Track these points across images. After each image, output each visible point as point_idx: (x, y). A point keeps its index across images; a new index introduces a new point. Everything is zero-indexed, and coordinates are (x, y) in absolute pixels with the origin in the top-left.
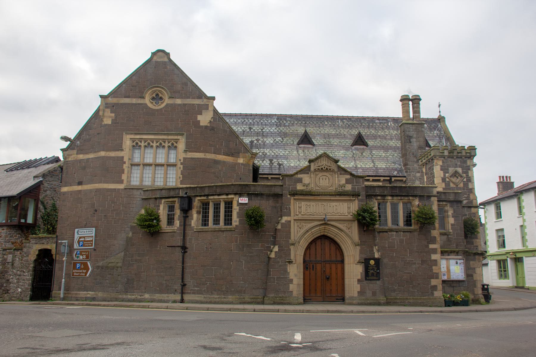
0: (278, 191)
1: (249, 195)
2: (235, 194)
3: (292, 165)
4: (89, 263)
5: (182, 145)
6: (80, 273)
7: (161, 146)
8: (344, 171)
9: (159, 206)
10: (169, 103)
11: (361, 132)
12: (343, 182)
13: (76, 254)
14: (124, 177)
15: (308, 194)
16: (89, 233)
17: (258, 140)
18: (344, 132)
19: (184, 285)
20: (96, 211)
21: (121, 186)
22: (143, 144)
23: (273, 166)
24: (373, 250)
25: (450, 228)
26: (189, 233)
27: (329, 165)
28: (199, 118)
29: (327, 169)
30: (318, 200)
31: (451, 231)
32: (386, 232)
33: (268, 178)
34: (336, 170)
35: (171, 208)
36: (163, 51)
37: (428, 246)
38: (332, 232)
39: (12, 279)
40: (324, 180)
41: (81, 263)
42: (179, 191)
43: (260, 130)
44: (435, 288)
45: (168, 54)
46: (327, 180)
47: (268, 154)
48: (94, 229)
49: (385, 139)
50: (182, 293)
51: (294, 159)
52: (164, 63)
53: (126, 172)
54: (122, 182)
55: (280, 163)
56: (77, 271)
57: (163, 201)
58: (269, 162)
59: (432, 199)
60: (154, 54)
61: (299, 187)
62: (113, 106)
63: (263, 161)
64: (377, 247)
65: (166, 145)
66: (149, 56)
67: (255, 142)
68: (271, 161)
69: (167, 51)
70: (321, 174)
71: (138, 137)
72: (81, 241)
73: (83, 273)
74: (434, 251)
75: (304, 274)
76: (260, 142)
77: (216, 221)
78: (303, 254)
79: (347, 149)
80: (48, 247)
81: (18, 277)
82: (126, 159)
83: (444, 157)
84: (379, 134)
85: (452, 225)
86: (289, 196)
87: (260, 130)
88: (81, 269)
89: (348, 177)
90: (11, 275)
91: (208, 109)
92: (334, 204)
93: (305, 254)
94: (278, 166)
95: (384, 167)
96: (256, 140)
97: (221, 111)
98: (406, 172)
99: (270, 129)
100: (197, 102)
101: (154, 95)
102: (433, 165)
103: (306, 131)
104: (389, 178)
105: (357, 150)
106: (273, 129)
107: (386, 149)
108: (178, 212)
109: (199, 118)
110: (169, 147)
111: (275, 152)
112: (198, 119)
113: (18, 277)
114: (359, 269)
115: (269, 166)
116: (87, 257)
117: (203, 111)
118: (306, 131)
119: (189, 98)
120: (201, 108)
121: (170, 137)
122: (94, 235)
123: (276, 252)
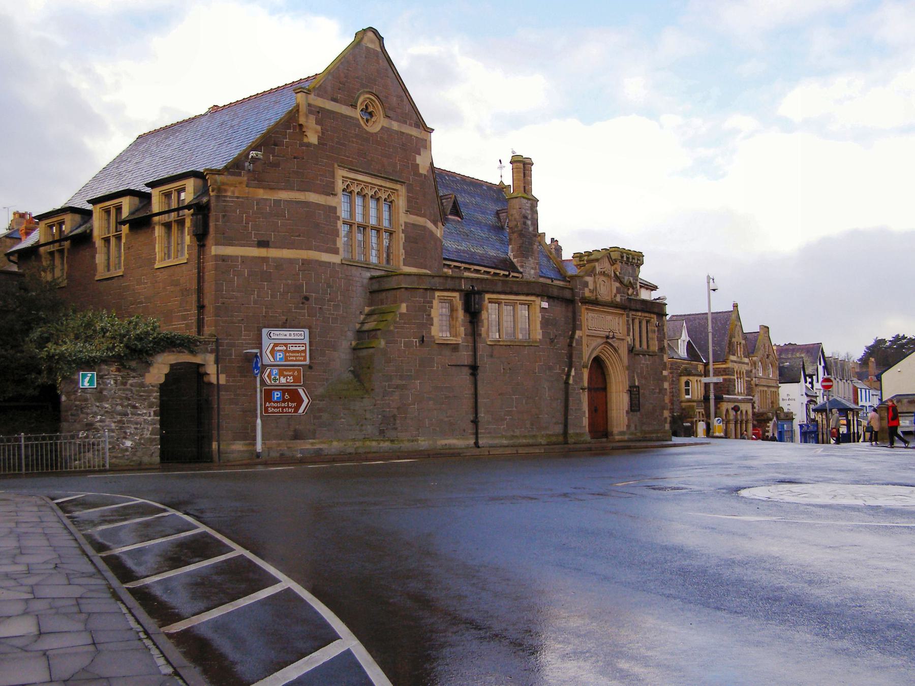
0: (567, 294)
2: (537, 296)
4: (301, 391)
5: (401, 203)
6: (283, 408)
9: (432, 303)
15: (594, 303)
19: (475, 422)
20: (307, 298)
21: (335, 259)
26: (480, 346)
30: (608, 312)
36: (375, 32)
39: (101, 421)
41: (284, 392)
42: (461, 282)
45: (381, 39)
48: (307, 331)
50: (476, 434)
54: (336, 251)
56: (275, 405)
57: (437, 294)
61: (587, 294)
72: (279, 351)
73: (288, 407)
80: (197, 360)
81: (119, 418)
88: (284, 401)
90: (95, 414)
92: (609, 317)
98: (522, 266)
112: (418, 162)
113: (119, 418)
114: (625, 398)
116: (296, 379)
117: (422, 150)
122: (307, 341)
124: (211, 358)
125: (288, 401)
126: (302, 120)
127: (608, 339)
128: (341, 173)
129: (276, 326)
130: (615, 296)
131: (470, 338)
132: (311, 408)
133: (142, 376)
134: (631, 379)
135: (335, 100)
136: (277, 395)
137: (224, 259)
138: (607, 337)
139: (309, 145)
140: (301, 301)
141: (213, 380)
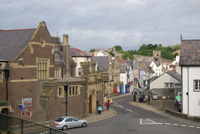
4: (30, 112)
5: (49, 62)
13: (24, 109)
15: (90, 84)
16: (29, 100)
20: (31, 91)
35: (60, 89)
36: (44, 22)
41: (26, 113)
45: (45, 23)
48: (31, 98)
54: (36, 78)
57: (59, 87)
77: (73, 94)
82: (37, 69)
98: (66, 64)
116: (29, 110)
122: (31, 100)
124: (11, 106)
126: (30, 49)
127: (93, 91)
128: (37, 59)
129: (25, 98)
131: (66, 96)
132: (32, 116)
134: (97, 99)
135: (36, 42)
136: (25, 113)
137: (14, 83)
138: (93, 91)
139: (32, 54)
140: (31, 90)
141: (11, 111)
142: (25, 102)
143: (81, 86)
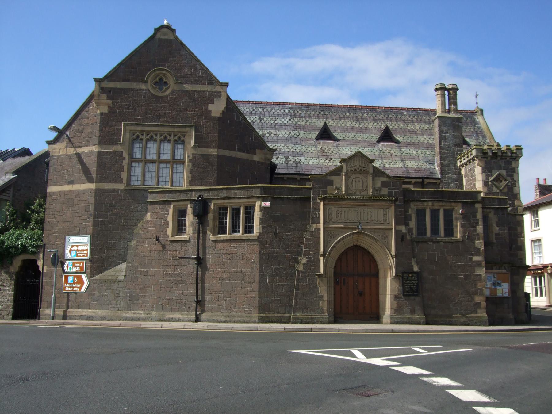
1: (273, 200)
2: (258, 197)
3: (311, 163)
6: (73, 287)
7: (165, 140)
8: (378, 172)
10: (175, 89)
11: (388, 125)
12: (379, 185)
14: (124, 175)
17: (270, 133)
18: (371, 125)
21: (121, 186)
22: (144, 137)
23: (289, 165)
24: (411, 263)
25: (494, 239)
27: (363, 165)
28: (211, 107)
29: (361, 170)
31: (495, 241)
32: (426, 242)
33: (283, 178)
34: (371, 171)
37: (471, 259)
38: (366, 243)
40: (357, 182)
41: (75, 277)
43: (272, 122)
44: (478, 305)
45: (173, 31)
46: (361, 182)
47: (283, 150)
49: (416, 134)
51: (314, 158)
52: (170, 41)
53: (126, 169)
54: (121, 181)
55: (297, 160)
58: (284, 160)
59: (477, 205)
60: (157, 30)
62: (110, 92)
63: (277, 158)
64: (415, 259)
65: (172, 138)
66: (151, 33)
67: (268, 135)
68: (286, 158)
69: (173, 27)
70: (354, 176)
71: (140, 128)
73: (76, 287)
74: (478, 264)
75: (335, 289)
76: (272, 135)
77: (235, 229)
78: (333, 267)
79: (373, 146)
82: (125, 155)
83: (487, 158)
84: (408, 128)
85: (496, 234)
86: (318, 201)
87: (272, 122)
88: (74, 283)
89: (385, 179)
91: (220, 97)
93: (335, 267)
94: (295, 165)
95: (416, 167)
96: (268, 133)
97: (233, 98)
99: (283, 120)
100: (207, 88)
101: (157, 80)
102: (475, 167)
103: (325, 123)
104: (421, 180)
105: (385, 146)
106: (287, 121)
107: (417, 146)
108: (190, 218)
109: (211, 107)
110: (175, 141)
111: (290, 147)
112: (209, 109)
115: (285, 165)
116: (81, 269)
117: (215, 99)
118: (325, 123)
119: (198, 83)
120: (211, 97)
121: (176, 130)
123: (304, 264)
125: (76, 283)
130: (380, 189)
133: (9, 267)
135: (124, 81)
142: (72, 246)
143: (268, 204)
